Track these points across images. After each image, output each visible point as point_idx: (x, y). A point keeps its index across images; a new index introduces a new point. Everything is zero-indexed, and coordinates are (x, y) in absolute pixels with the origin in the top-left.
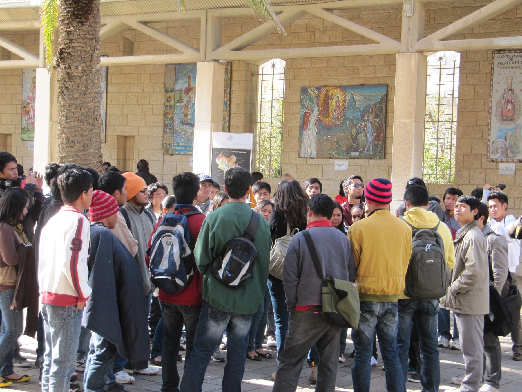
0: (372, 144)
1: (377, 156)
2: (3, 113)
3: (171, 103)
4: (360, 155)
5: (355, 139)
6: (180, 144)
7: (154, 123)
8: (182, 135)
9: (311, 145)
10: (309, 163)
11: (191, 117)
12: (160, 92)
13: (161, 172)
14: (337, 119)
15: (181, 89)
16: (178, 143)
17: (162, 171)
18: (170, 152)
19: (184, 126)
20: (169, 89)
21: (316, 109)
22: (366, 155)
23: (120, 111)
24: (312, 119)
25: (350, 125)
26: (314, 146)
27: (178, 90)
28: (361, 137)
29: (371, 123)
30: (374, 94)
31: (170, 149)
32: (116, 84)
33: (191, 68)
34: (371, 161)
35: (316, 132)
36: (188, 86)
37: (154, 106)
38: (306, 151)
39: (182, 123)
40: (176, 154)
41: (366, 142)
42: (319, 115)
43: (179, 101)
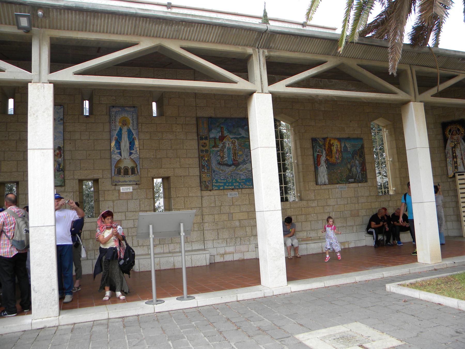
0: (360, 174)
1: (364, 181)
2: (4, 160)
3: (207, 148)
4: (354, 181)
5: (350, 170)
6: (219, 180)
7: (189, 165)
8: (220, 173)
9: (324, 176)
10: (323, 188)
11: (227, 159)
12: (193, 139)
13: (200, 206)
14: (337, 159)
15: (215, 137)
16: (217, 180)
17: (201, 205)
18: (209, 189)
19: (222, 166)
20: (204, 137)
21: (324, 152)
22: (358, 180)
23: (153, 155)
24: (323, 159)
25: (346, 162)
26: (326, 176)
27: (213, 138)
28: (354, 169)
29: (358, 160)
30: (357, 143)
31: (210, 185)
32: (147, 132)
33: (223, 121)
34: (360, 184)
35: (326, 167)
36: (222, 135)
37: (188, 151)
38: (322, 180)
39: (219, 164)
40: (216, 190)
41: (357, 173)
42: (326, 156)
43: (214, 147)
